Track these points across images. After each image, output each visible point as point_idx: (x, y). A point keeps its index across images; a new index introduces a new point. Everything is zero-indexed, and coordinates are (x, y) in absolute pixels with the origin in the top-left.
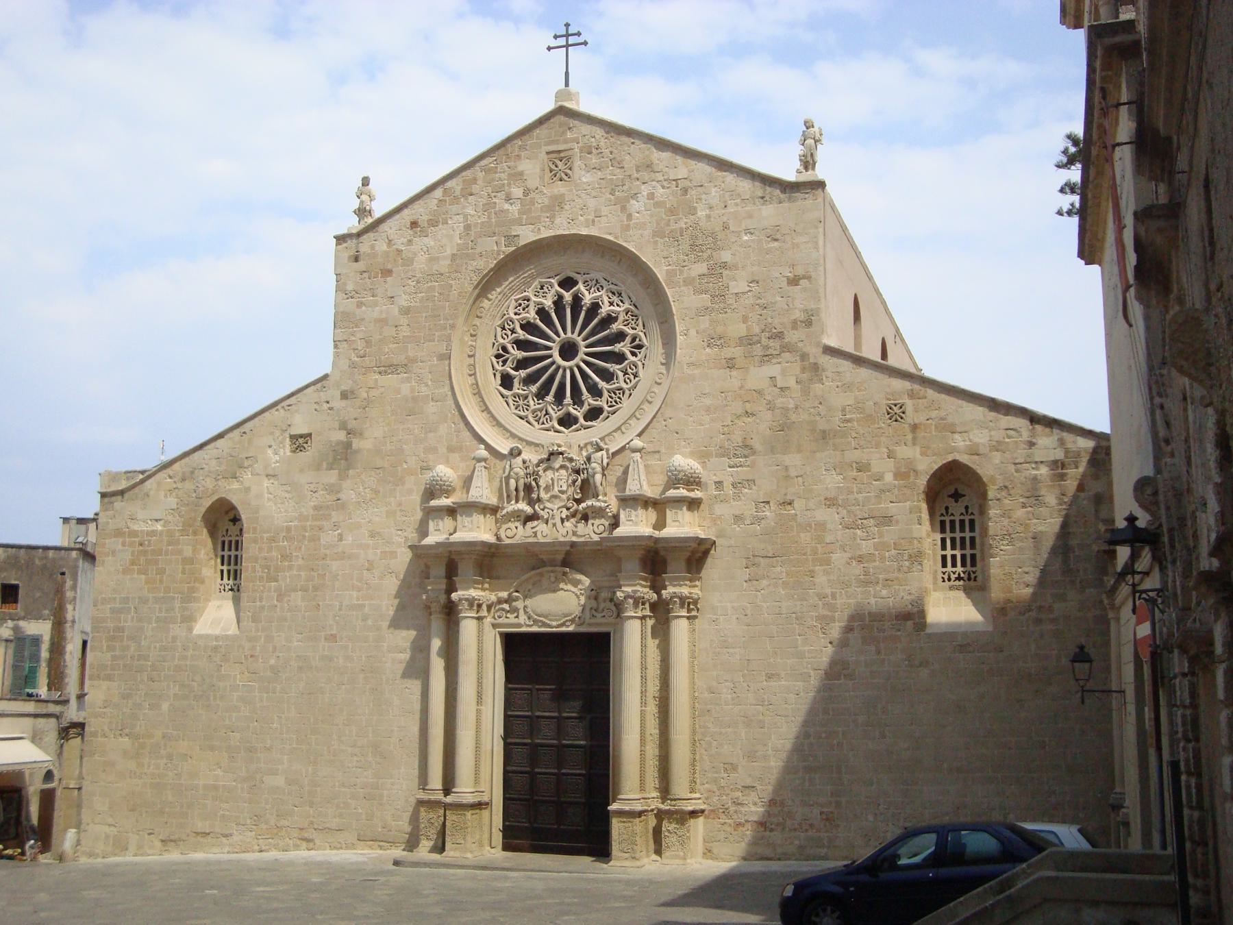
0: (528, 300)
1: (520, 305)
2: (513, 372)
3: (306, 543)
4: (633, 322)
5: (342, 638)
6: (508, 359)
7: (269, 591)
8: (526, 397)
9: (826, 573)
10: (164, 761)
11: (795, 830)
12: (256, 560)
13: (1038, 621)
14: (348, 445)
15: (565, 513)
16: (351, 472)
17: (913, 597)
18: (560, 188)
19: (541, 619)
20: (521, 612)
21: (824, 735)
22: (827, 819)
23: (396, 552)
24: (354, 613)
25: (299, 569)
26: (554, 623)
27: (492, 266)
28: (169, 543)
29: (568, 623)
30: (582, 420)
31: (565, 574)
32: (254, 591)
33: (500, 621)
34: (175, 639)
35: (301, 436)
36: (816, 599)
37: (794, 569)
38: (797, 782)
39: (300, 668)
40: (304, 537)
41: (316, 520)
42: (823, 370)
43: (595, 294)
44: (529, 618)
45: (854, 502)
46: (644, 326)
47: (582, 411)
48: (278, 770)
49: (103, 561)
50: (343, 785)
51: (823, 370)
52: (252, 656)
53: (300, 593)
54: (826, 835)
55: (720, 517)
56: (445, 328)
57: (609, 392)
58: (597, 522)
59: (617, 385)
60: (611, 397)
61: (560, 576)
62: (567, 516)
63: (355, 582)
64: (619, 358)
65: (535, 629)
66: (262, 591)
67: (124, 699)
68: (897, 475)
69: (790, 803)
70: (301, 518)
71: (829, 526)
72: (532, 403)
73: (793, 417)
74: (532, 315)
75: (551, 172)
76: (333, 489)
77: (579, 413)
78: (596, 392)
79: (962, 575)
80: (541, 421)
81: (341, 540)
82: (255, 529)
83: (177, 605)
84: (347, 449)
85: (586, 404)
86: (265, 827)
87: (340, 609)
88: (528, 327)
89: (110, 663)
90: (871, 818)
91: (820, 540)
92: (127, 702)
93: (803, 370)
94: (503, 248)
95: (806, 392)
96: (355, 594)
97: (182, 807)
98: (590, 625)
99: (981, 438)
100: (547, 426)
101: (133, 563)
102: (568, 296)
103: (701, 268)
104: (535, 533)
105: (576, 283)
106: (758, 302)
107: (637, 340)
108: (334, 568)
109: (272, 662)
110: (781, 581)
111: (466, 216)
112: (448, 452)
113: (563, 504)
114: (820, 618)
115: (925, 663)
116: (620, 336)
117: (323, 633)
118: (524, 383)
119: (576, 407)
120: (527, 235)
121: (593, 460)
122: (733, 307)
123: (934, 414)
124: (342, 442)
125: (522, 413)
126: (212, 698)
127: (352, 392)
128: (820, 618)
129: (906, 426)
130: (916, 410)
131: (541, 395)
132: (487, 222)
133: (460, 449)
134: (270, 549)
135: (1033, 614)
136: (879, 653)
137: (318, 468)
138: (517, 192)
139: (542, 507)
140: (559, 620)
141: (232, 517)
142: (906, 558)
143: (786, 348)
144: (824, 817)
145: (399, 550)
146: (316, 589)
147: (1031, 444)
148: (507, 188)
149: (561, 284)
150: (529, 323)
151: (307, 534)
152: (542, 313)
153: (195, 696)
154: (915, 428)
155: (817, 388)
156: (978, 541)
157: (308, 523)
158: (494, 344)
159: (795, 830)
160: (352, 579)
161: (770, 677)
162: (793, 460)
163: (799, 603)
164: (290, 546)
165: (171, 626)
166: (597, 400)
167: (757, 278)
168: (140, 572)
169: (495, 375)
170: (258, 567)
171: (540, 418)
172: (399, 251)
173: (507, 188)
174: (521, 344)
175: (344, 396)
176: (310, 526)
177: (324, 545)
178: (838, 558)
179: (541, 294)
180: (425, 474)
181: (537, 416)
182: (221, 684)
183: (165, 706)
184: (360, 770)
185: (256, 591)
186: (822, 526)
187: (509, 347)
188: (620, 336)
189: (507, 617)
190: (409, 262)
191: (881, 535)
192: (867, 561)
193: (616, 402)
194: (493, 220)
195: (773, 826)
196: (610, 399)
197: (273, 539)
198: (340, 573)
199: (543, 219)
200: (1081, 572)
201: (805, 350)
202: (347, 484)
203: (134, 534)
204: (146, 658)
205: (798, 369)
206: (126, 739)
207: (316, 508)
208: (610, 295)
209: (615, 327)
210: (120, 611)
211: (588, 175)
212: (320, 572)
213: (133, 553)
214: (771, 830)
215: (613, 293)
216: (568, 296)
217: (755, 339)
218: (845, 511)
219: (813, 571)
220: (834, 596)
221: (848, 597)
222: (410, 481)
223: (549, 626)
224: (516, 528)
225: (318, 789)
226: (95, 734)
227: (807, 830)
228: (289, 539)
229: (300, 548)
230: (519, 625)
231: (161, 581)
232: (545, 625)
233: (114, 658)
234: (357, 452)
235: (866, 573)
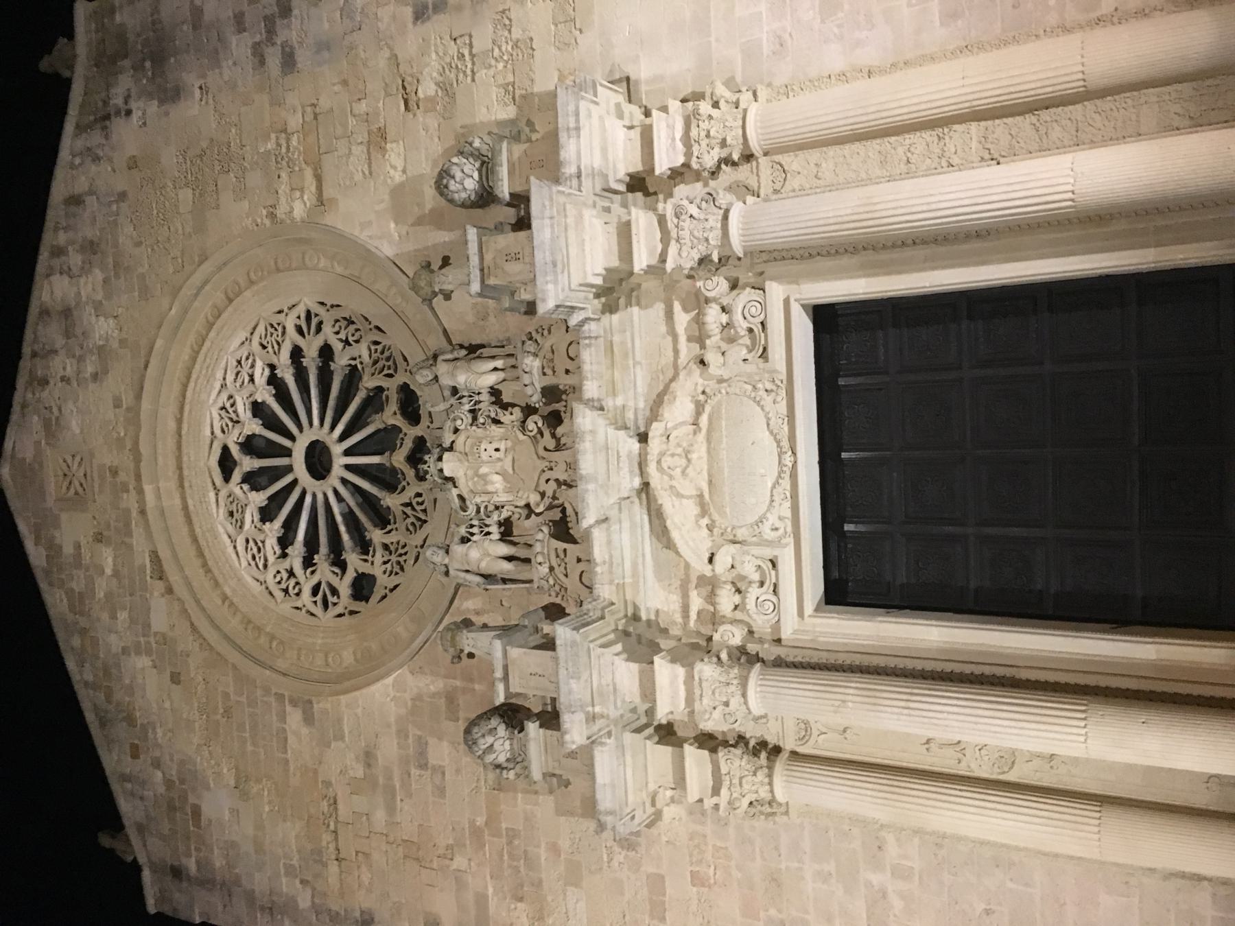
2: (350, 575)
8: (386, 547)
30: (417, 431)
46: (280, 312)
47: (404, 430)
57: (373, 374)
62: (553, 435)
64: (326, 352)
78: (375, 400)
80: (423, 518)
85: (391, 421)
102: (248, 464)
118: (367, 554)
119: (398, 442)
131: (382, 519)
139: (538, 498)
149: (227, 478)
166: (387, 397)
171: (419, 519)
172: (169, 784)
174: (308, 562)
181: (413, 524)
193: (388, 359)
215: (237, 374)
224: (579, 560)
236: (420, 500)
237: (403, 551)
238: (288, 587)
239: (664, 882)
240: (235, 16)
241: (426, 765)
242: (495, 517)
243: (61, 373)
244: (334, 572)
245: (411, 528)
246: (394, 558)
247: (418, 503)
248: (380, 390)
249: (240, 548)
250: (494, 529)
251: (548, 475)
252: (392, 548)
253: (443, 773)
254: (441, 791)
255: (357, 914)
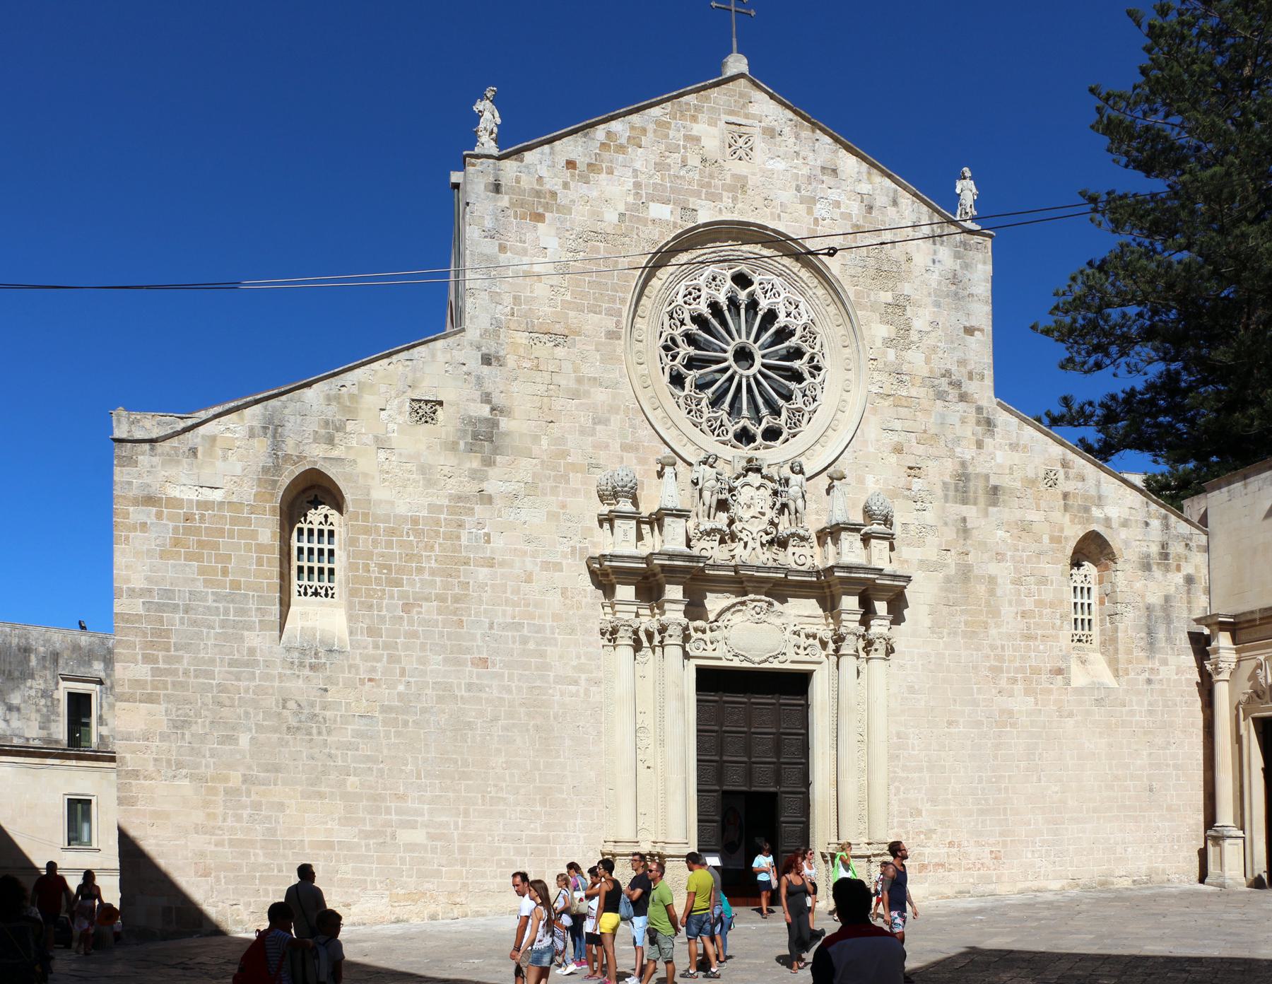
0: (699, 290)
1: (690, 294)
3: (441, 541)
4: (811, 340)
5: (494, 665)
6: (678, 353)
7: (392, 597)
9: (998, 626)
10: (249, 811)
11: (969, 869)
12: (369, 555)
13: (1149, 681)
14: (495, 424)
15: (766, 538)
16: (498, 458)
17: (1064, 653)
18: (741, 168)
19: (743, 653)
20: (722, 643)
21: (994, 780)
22: (996, 858)
23: (560, 563)
24: (510, 634)
25: (433, 573)
26: (757, 659)
27: (670, 239)
28: (234, 521)
29: (771, 659)
30: (759, 439)
31: (771, 604)
32: (368, 596)
33: (698, 653)
34: (252, 651)
35: (427, 402)
36: (988, 649)
37: (970, 619)
38: (972, 824)
39: (440, 699)
40: (437, 533)
41: (452, 514)
42: (995, 426)
43: (771, 300)
44: (729, 651)
45: (1019, 559)
48: (416, 822)
49: (127, 538)
50: (504, 840)
51: (995, 426)
52: (370, 680)
53: (435, 603)
54: (995, 872)
55: (907, 561)
56: (614, 302)
58: (798, 551)
59: (795, 406)
60: (798, 420)
61: (765, 605)
63: (508, 595)
65: (736, 663)
66: (381, 598)
67: (177, 728)
68: (1053, 539)
69: (966, 844)
70: (432, 508)
71: (1000, 581)
72: (705, 410)
73: (970, 470)
74: (704, 310)
75: (730, 147)
76: (475, 475)
77: (758, 431)
79: (1082, 638)
81: (488, 541)
82: (366, 515)
83: (252, 606)
84: (492, 428)
85: (764, 421)
86: (403, 892)
87: (491, 627)
88: (699, 320)
89: (149, 678)
90: (1029, 855)
91: (992, 592)
92: (183, 734)
93: (978, 423)
94: (679, 221)
95: (980, 445)
96: (509, 609)
97: (280, 871)
98: (792, 662)
99: (1113, 512)
100: (723, 438)
101: (176, 542)
103: (887, 297)
104: (733, 557)
105: (750, 283)
106: (939, 344)
107: (816, 360)
108: (481, 577)
109: (401, 688)
110: (960, 630)
111: (635, 171)
112: (622, 450)
113: (763, 527)
114: (993, 669)
115: (1071, 715)
116: (797, 353)
117: (469, 656)
120: (705, 215)
121: (792, 482)
122: (917, 345)
123: (1080, 485)
124: (487, 420)
125: (695, 419)
126: (314, 731)
127: (498, 359)
128: (992, 669)
129: (1060, 492)
130: (1067, 477)
131: (715, 403)
132: (661, 185)
133: (637, 450)
134: (389, 544)
135: (1146, 675)
136: (1037, 704)
137: (453, 447)
138: (694, 161)
140: (764, 655)
141: (312, 498)
142: (1058, 617)
143: (963, 398)
144: (993, 856)
145: (564, 562)
146: (457, 599)
147: (1147, 524)
148: (682, 151)
150: (700, 315)
151: (441, 530)
152: (714, 306)
153: (289, 728)
154: (1065, 496)
155: (988, 441)
156: (1093, 607)
157: (442, 516)
158: (661, 333)
159: (969, 869)
160: (505, 592)
161: (950, 723)
162: (970, 511)
163: (975, 653)
164: (418, 542)
165: (246, 633)
166: (776, 419)
167: (937, 320)
168: (189, 557)
169: (663, 368)
170: (372, 567)
172: (554, 194)
173: (682, 151)
175: (487, 360)
176: (445, 519)
177: (466, 547)
178: (1007, 611)
179: (714, 286)
180: (594, 473)
182: (328, 714)
183: (244, 740)
184: (524, 821)
185: (372, 597)
186: (992, 580)
187: (679, 340)
188: (797, 353)
189: (704, 649)
190: (565, 210)
191: (1039, 591)
192: (1029, 618)
193: (795, 423)
194: (668, 185)
195: (951, 867)
196: (789, 421)
197: (392, 532)
198: (489, 582)
199: (725, 199)
200: (1178, 642)
201: (979, 403)
202: (492, 472)
203: (174, 503)
204: (210, 675)
205: (974, 420)
206: (186, 782)
207: (451, 497)
208: (787, 304)
209: (793, 342)
210: (161, 607)
211: (771, 162)
212: (462, 579)
213: (176, 529)
214: (950, 870)
215: (790, 303)
216: (743, 295)
217: (936, 382)
218: (1012, 567)
219: (986, 623)
220: (1003, 647)
221: (1014, 651)
222: (576, 479)
223: (751, 661)
224: (712, 548)
225: (473, 845)
226: (135, 774)
227: (979, 869)
228: (418, 533)
229: (432, 547)
230: (720, 659)
231: (225, 572)
232: (747, 659)
233: (155, 672)
234: (506, 434)
235: (1029, 628)
236: (725, 432)
237: (698, 415)
238: (674, 319)
239: (559, 571)
240: (965, 360)
241: (595, 424)
242: (730, 501)
243: (802, 154)
244: (684, 359)
245: (710, 423)
246: (694, 407)
247: (723, 431)
248: (779, 414)
249: (694, 282)
250: (722, 497)
251: (750, 536)
252: (699, 407)
253: (592, 435)
254: (583, 432)
255: (502, 353)
